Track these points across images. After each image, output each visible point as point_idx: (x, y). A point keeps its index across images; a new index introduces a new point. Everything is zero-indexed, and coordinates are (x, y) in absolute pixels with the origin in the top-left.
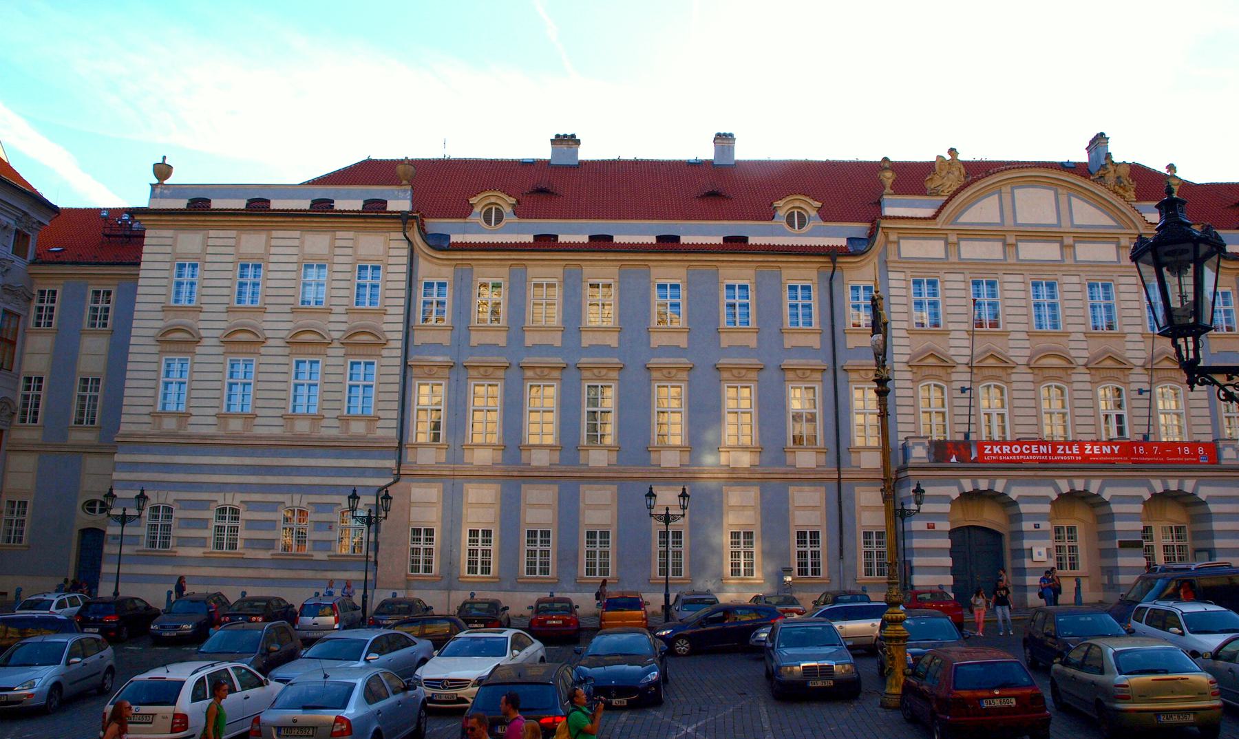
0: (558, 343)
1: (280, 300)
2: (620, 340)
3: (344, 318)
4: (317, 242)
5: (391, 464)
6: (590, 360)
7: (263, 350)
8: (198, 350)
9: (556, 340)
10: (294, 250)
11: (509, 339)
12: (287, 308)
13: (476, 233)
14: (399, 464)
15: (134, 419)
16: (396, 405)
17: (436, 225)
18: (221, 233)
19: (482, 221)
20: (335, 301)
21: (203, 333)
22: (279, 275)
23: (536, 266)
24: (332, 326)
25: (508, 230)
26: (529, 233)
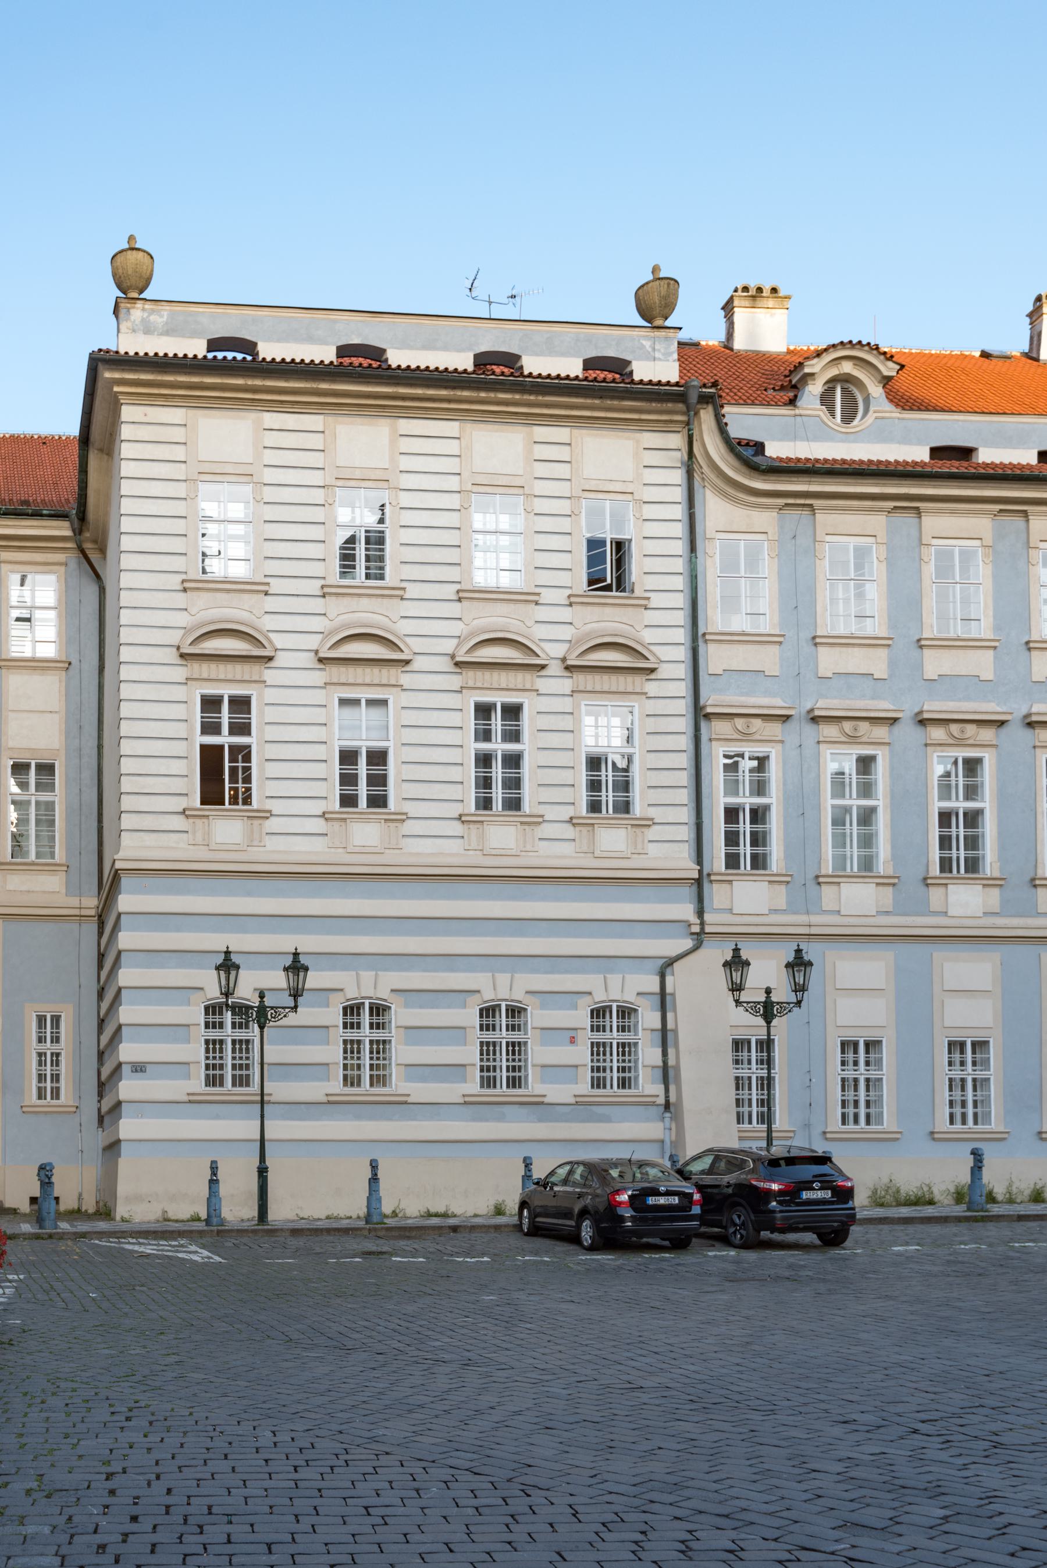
0: (988, 674)
1: (431, 573)
3: (566, 614)
5: (686, 911)
7: (406, 680)
8: (270, 675)
10: (452, 465)
11: (892, 664)
13: (816, 439)
14: (700, 913)
15: (148, 822)
16: (684, 796)
17: (745, 421)
18: (291, 420)
19: (822, 412)
21: (279, 641)
22: (424, 518)
24: (542, 631)
25: (882, 437)
26: (920, 443)
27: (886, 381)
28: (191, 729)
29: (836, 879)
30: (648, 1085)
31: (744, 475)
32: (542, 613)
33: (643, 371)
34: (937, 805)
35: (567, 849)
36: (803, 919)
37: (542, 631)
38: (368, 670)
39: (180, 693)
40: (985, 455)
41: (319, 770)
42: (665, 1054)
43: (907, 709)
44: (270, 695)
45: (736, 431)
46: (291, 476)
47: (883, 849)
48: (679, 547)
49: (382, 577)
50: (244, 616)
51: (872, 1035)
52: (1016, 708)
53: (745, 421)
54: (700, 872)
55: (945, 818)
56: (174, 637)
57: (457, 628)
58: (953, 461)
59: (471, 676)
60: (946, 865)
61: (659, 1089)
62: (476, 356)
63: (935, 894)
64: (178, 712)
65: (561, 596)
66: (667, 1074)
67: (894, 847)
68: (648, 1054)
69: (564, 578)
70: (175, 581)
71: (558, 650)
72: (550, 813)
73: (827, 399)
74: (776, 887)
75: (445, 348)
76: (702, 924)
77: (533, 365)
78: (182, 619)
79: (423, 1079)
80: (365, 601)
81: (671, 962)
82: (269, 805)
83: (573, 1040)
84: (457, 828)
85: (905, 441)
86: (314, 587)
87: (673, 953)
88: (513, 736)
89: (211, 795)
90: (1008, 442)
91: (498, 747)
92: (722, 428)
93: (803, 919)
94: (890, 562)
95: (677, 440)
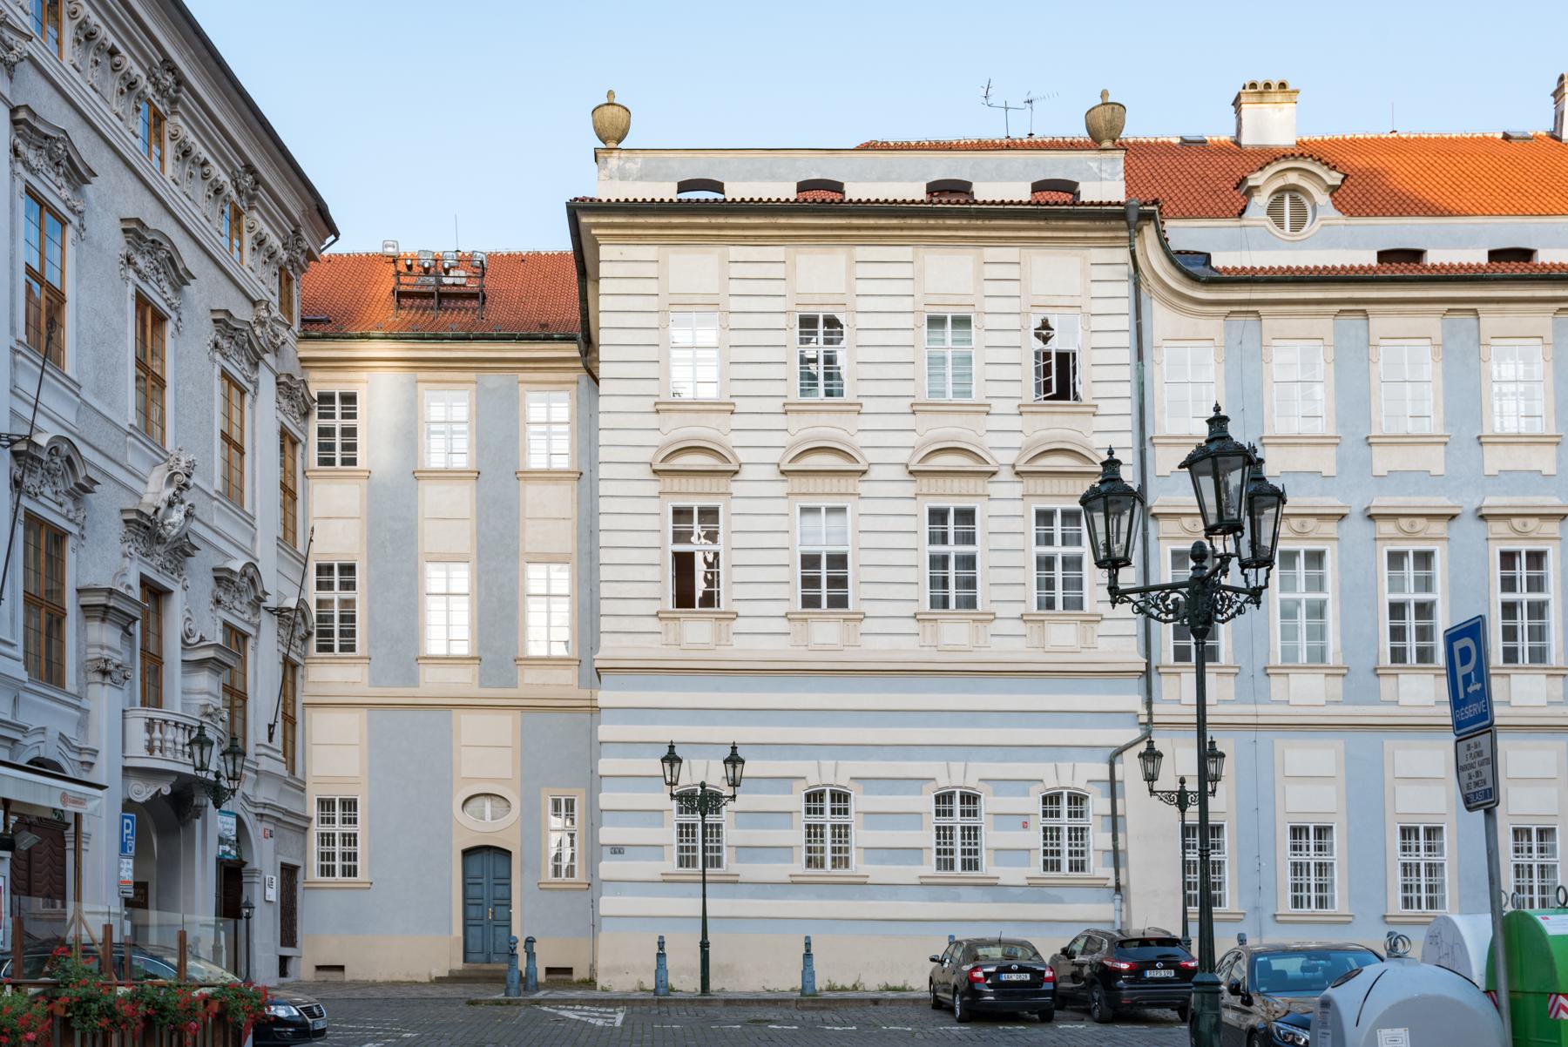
0: (1438, 469)
1: (886, 388)
2: (1559, 461)
3: (1016, 423)
4: (949, 269)
5: (1136, 702)
6: (1505, 500)
7: (863, 488)
8: (736, 487)
9: (1433, 460)
10: (905, 287)
11: (1341, 461)
12: (904, 405)
14: (1149, 704)
20: (995, 389)
21: (743, 456)
23: (1387, 313)
24: (994, 440)
25: (1330, 244)
26: (1367, 247)
27: (1333, 190)
28: (664, 539)
29: (1284, 671)
30: (1099, 868)
31: (1186, 286)
32: (993, 423)
33: (1090, 192)
34: (1387, 597)
35: (1018, 644)
36: (1251, 709)
37: (994, 440)
38: (827, 480)
39: (653, 505)
40: (1433, 258)
41: (782, 574)
42: (1115, 838)
43: (1355, 506)
44: (736, 506)
45: (1175, 245)
46: (754, 305)
47: (1333, 641)
48: (1128, 356)
49: (841, 394)
50: (712, 433)
51: (1323, 821)
52: (1467, 502)
53: (1185, 233)
54: (1148, 665)
55: (1397, 610)
56: (648, 455)
57: (911, 439)
58: (1402, 264)
59: (925, 484)
60: (1398, 655)
61: (1110, 872)
62: (929, 185)
63: (1386, 684)
64: (652, 522)
65: (1012, 406)
66: (1117, 857)
67: (1343, 638)
68: (1099, 839)
69: (1014, 390)
70: (648, 404)
71: (1009, 457)
72: (1001, 611)
73: (1274, 210)
74: (1225, 678)
75: (899, 179)
76: (1150, 714)
77: (984, 192)
78: (656, 439)
79: (882, 862)
80: (824, 416)
81: (1120, 751)
82: (736, 607)
83: (1025, 825)
84: (912, 626)
85: (1353, 246)
86: (777, 405)
87: (1123, 743)
88: (969, 539)
89: (684, 598)
90: (1459, 244)
91: (952, 549)
92: (1163, 242)
93: (1251, 709)
94: (1338, 363)
95: (1123, 255)
